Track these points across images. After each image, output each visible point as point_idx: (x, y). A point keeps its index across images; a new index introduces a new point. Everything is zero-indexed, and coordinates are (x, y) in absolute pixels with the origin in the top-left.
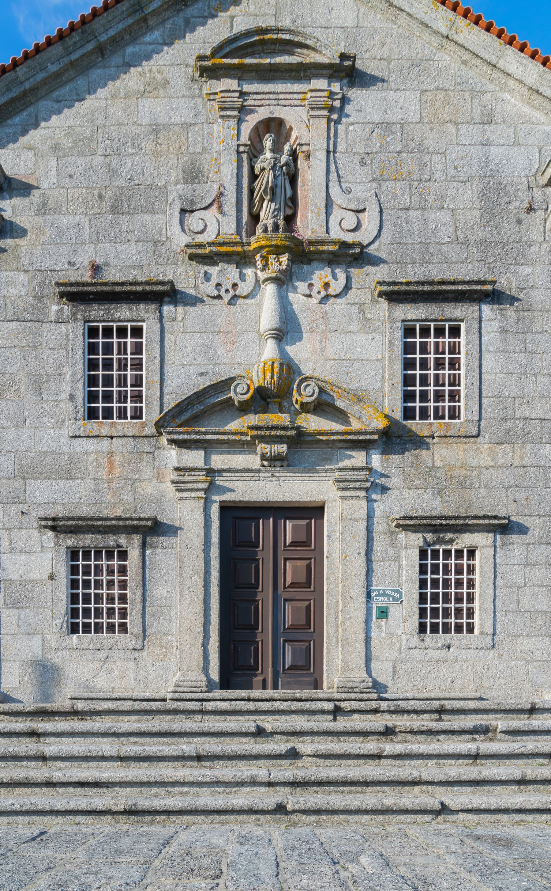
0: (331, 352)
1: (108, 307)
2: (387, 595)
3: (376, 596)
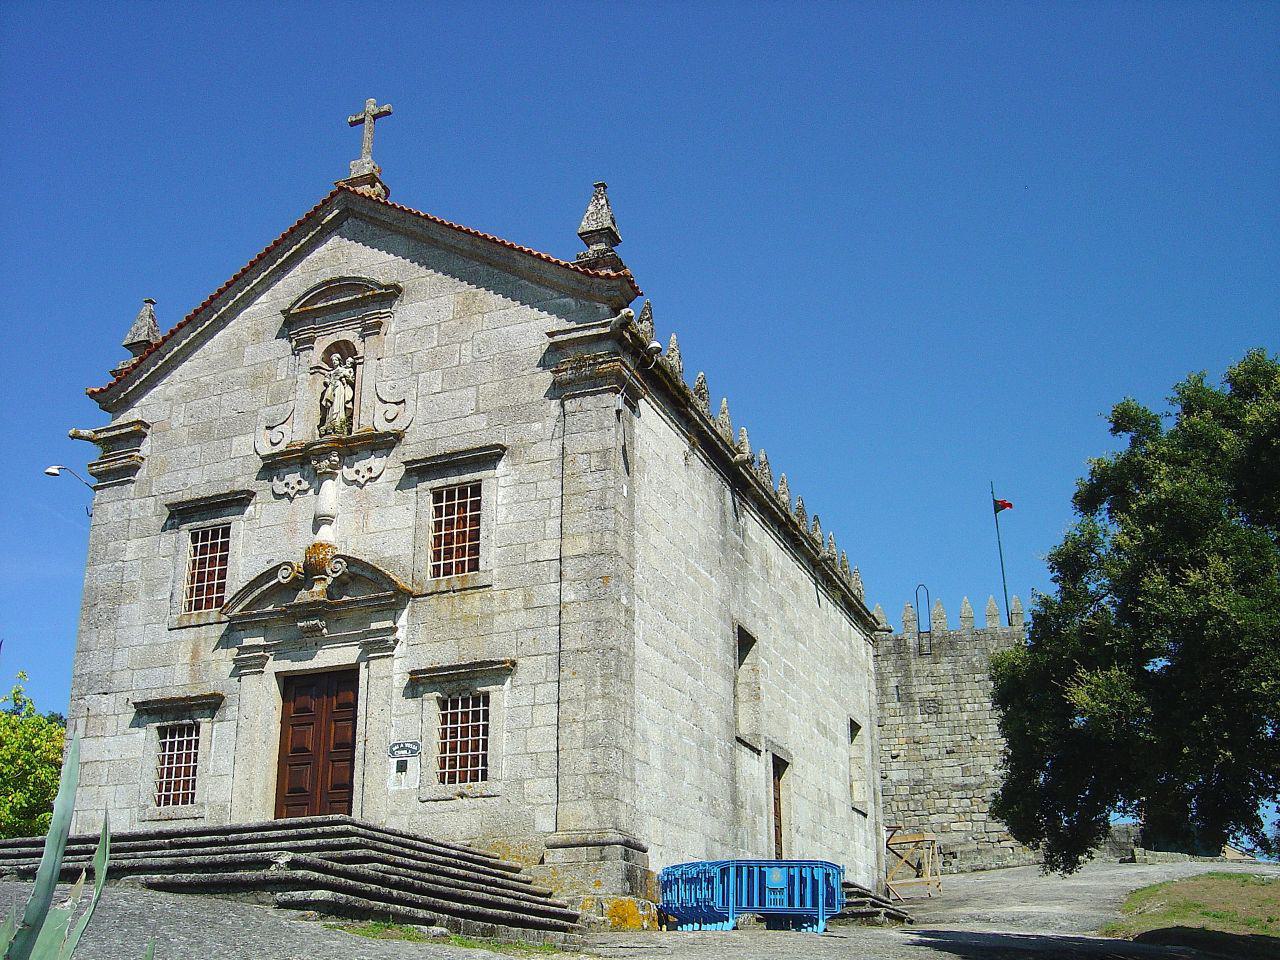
0: (372, 526)
1: (205, 517)
2: (408, 749)
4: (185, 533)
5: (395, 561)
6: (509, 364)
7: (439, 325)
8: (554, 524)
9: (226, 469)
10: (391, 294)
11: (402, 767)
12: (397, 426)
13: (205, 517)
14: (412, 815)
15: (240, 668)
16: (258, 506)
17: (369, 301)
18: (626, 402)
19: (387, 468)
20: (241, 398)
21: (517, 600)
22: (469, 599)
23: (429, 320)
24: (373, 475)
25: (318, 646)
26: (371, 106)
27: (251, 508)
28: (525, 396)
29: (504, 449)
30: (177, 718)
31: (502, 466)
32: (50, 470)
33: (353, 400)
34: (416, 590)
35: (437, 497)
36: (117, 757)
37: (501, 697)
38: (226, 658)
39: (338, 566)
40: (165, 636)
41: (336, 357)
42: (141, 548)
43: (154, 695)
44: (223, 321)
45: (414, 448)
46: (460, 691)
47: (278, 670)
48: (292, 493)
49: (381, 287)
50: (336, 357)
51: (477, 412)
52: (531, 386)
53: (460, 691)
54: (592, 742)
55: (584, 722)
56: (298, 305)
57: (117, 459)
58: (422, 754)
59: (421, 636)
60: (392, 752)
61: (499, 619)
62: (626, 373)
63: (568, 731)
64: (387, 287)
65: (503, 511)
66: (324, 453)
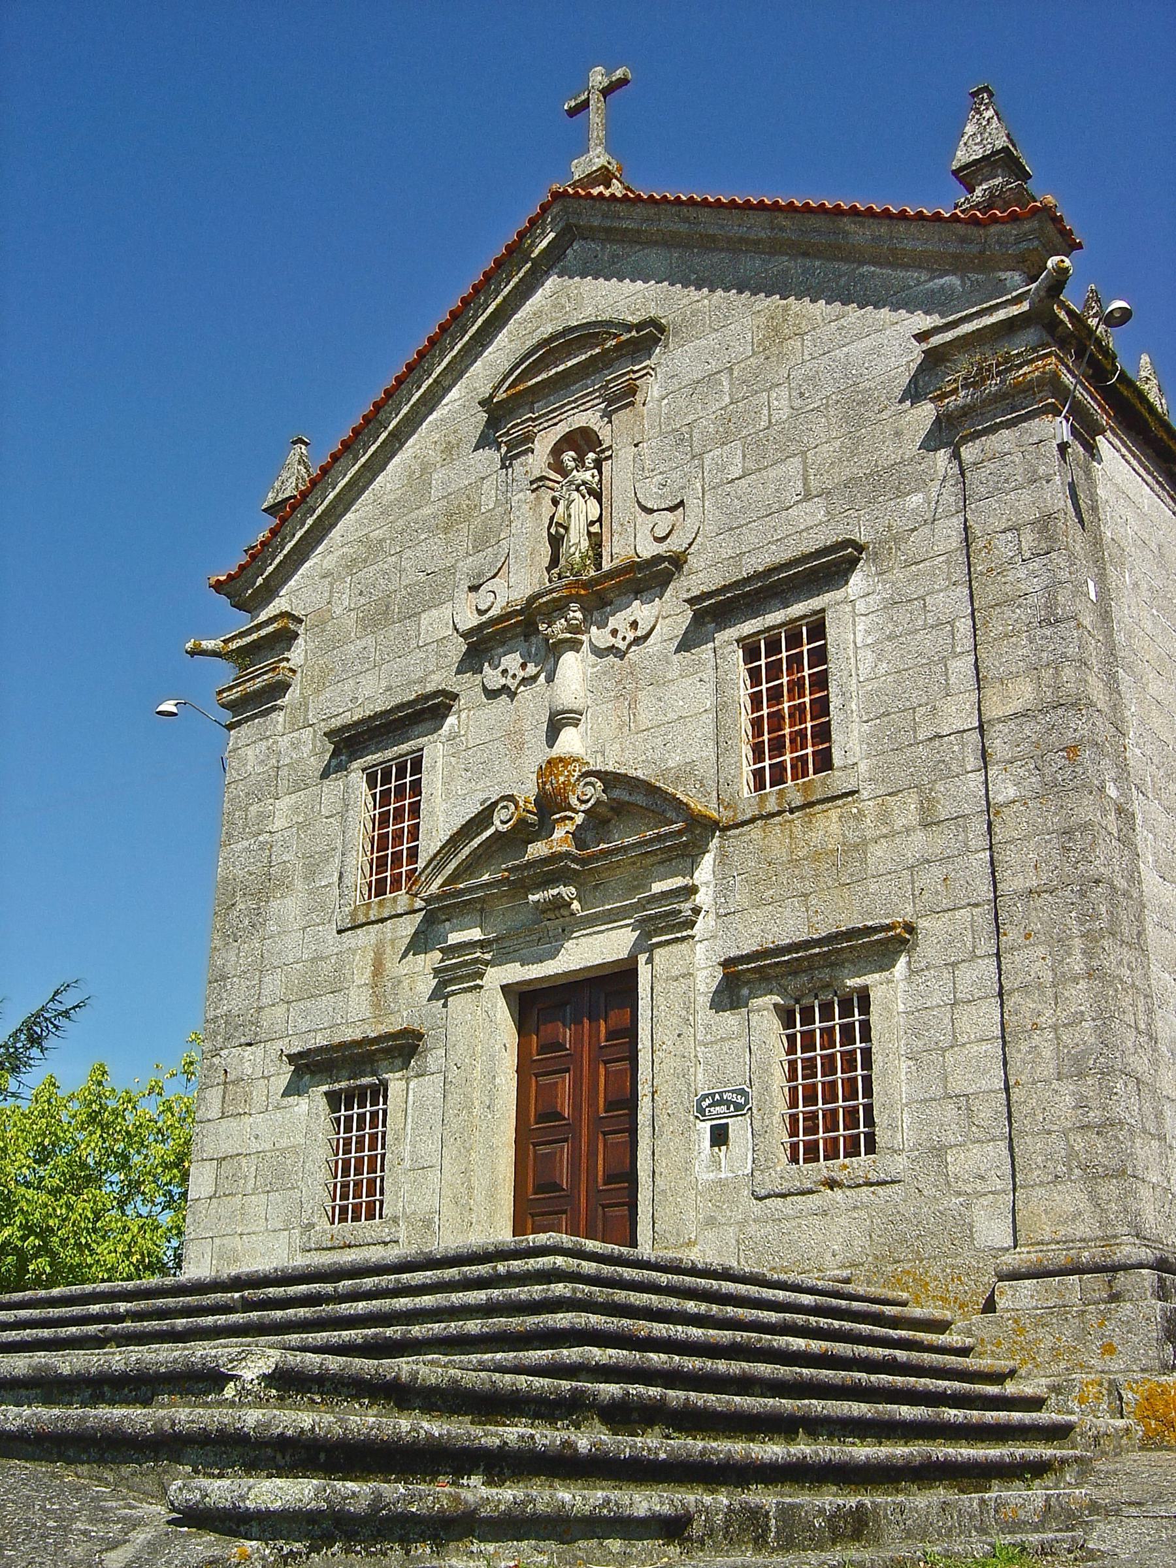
1: (384, 742)
2: (728, 1103)
3: (709, 1106)
4: (356, 778)
5: (687, 771)
6: (855, 406)
7: (731, 369)
8: (962, 667)
10: (647, 337)
11: (720, 1136)
12: (675, 544)
13: (384, 742)
14: (742, 1224)
15: (446, 984)
16: (464, 715)
17: (612, 356)
18: (1074, 432)
19: (662, 616)
20: (432, 550)
21: (907, 812)
22: (820, 822)
23: (714, 366)
24: (639, 633)
25: (566, 933)
26: (598, 78)
27: (451, 720)
28: (889, 453)
29: (860, 548)
31: (857, 581)
32: (161, 708)
33: (600, 520)
34: (725, 816)
35: (751, 654)
36: (268, 1146)
37: (891, 990)
39: (590, 790)
41: (568, 457)
42: (296, 810)
44: (398, 439)
45: (703, 576)
46: (815, 988)
47: (504, 982)
48: (512, 684)
49: (629, 327)
50: (568, 457)
51: (807, 497)
52: (898, 434)
53: (815, 988)
54: (1075, 1067)
55: (1055, 1028)
56: (504, 388)
58: (755, 1111)
59: (740, 897)
60: (701, 1111)
61: (878, 851)
62: (1068, 379)
63: (1024, 1047)
64: (639, 327)
65: (868, 656)
66: (558, 608)
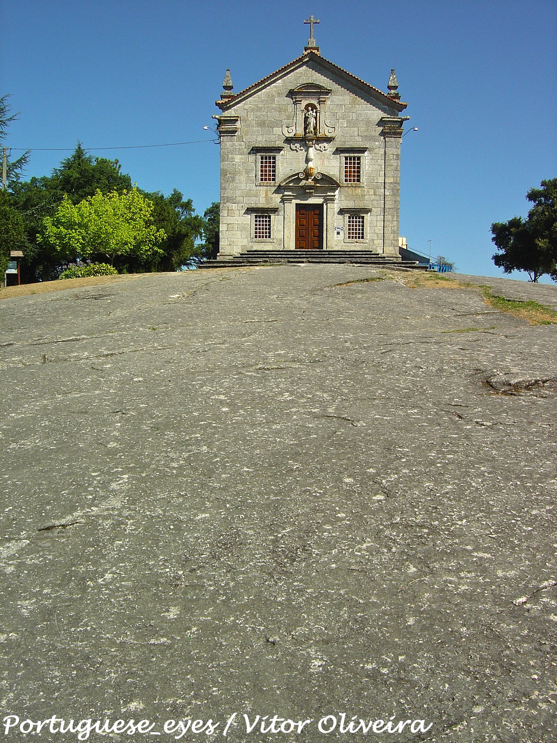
4: (259, 156)
6: (368, 122)
9: (273, 138)
10: (328, 92)
11: (338, 233)
13: (267, 154)
15: (283, 201)
17: (321, 92)
19: (329, 148)
21: (372, 192)
25: (310, 197)
27: (282, 152)
28: (373, 133)
30: (262, 214)
37: (367, 217)
38: (277, 198)
40: (254, 188)
43: (253, 206)
46: (356, 214)
49: (327, 89)
50: (310, 108)
51: (358, 136)
53: (356, 214)
57: (225, 128)
59: (343, 198)
61: (366, 197)
64: (329, 90)
65: (367, 167)
